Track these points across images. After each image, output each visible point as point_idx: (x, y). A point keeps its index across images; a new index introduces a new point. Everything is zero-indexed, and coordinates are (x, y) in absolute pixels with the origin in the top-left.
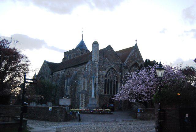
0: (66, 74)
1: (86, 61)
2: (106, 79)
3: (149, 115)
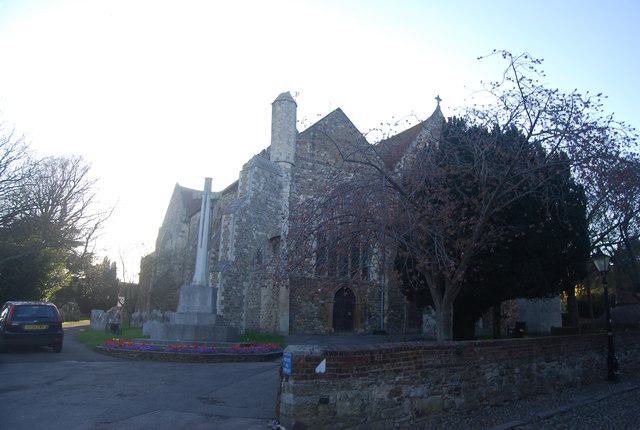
3: (380, 392)
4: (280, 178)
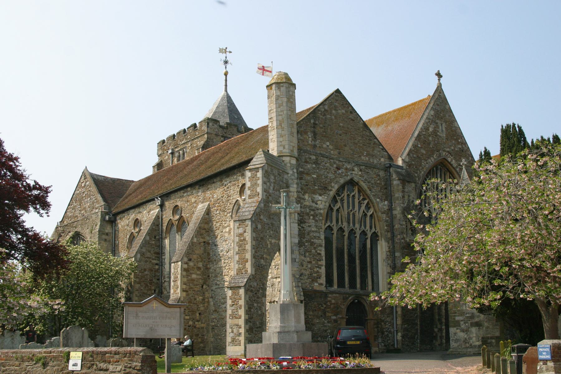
0: (168, 215)
1: (244, 158)
2: (330, 228)
4: (286, 176)
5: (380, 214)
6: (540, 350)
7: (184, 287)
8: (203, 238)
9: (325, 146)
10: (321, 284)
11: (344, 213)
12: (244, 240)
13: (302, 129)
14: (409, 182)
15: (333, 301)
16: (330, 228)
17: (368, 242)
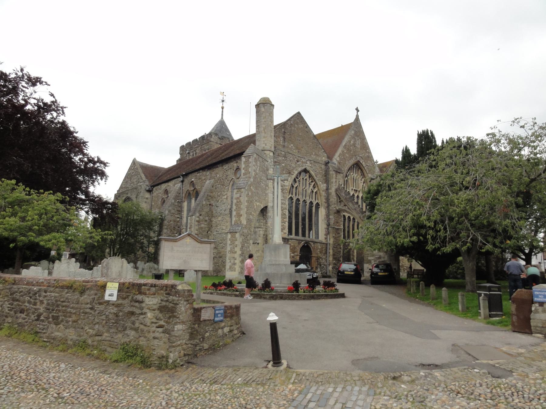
0: (187, 187)
1: (238, 152)
2: (291, 198)
4: (266, 163)
5: (321, 191)
6: (537, 293)
7: (196, 232)
8: (209, 202)
9: (290, 147)
10: (285, 233)
11: (300, 189)
12: (240, 201)
13: (277, 135)
14: (339, 173)
15: (292, 245)
16: (291, 198)
17: (314, 208)
